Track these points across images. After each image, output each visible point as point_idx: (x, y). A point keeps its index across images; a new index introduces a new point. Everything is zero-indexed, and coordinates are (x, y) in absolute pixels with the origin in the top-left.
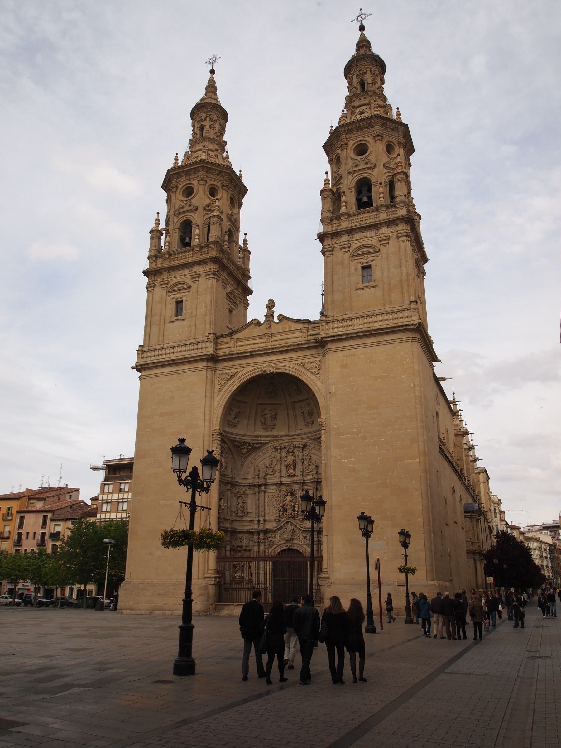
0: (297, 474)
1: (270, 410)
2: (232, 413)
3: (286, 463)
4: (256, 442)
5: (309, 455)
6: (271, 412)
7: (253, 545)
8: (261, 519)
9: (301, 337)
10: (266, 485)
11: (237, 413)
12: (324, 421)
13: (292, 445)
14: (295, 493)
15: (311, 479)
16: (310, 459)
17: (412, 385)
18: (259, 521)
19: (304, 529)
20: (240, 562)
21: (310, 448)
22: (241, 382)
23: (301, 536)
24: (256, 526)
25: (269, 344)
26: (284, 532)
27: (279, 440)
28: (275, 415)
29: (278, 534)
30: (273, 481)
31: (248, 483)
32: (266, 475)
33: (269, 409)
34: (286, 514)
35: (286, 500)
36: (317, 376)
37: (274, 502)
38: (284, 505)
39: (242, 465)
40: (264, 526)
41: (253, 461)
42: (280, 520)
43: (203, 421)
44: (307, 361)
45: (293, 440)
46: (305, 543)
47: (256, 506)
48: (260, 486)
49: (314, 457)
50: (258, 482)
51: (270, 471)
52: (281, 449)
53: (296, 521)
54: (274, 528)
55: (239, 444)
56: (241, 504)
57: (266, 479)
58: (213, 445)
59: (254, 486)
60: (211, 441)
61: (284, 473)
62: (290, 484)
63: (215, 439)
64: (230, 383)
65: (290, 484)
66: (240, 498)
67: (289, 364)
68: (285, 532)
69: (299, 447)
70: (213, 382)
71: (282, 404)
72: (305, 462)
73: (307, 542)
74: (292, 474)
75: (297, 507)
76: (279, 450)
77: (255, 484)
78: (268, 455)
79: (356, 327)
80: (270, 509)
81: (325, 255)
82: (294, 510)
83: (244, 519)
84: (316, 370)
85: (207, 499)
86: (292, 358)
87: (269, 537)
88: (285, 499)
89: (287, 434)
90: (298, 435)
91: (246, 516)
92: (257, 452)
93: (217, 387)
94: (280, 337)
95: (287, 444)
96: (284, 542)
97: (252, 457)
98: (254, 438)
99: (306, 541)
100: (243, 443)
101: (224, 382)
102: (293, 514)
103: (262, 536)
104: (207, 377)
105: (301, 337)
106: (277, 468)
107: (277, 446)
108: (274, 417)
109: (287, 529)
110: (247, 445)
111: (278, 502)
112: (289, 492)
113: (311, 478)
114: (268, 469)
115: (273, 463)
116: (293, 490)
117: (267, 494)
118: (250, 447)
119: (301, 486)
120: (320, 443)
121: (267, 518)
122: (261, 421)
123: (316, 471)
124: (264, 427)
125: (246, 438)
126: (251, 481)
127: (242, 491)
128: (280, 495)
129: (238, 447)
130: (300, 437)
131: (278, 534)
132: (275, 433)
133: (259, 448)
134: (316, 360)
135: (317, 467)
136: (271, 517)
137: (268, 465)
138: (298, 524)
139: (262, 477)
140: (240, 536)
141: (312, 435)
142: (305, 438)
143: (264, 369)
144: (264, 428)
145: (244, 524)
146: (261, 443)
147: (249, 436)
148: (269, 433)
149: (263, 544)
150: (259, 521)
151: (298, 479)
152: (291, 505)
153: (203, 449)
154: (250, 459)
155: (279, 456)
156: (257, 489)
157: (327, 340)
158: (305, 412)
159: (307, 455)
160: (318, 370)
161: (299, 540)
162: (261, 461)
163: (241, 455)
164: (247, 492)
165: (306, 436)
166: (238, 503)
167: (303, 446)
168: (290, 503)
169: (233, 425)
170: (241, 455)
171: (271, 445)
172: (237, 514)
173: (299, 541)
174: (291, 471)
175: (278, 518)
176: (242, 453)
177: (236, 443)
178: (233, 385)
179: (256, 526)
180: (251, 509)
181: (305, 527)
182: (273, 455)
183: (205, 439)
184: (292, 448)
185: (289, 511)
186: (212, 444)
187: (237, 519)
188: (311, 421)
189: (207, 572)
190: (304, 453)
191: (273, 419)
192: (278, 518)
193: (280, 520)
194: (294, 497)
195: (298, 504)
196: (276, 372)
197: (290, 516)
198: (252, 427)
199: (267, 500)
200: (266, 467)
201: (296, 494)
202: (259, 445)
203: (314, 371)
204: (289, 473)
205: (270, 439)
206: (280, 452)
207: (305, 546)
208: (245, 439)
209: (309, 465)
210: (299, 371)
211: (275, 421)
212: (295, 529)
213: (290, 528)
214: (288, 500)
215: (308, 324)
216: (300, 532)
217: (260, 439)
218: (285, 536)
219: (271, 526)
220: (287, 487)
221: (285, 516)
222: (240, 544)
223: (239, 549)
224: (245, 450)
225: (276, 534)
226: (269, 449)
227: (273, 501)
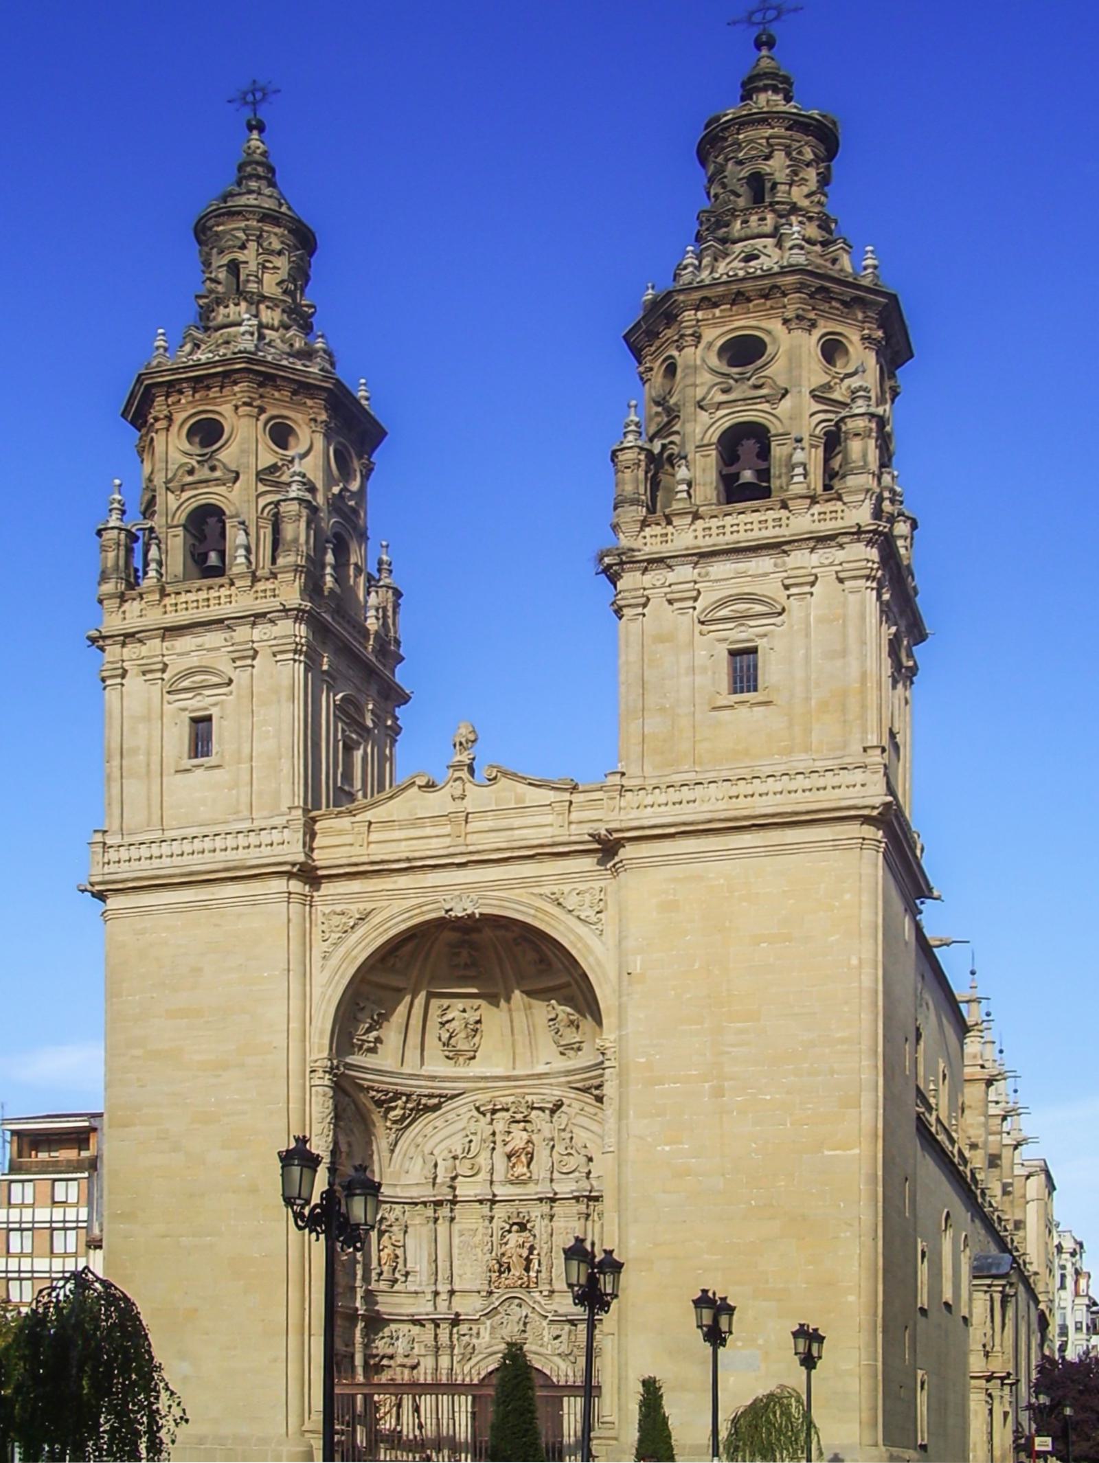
3: (508, 1149)
4: (426, 1092)
5: (568, 1129)
7: (423, 1352)
8: (443, 1288)
9: (551, 825)
10: (454, 1202)
13: (523, 1101)
15: (572, 1192)
17: (854, 961)
20: (390, 1394)
21: (572, 1111)
23: (545, 1333)
24: (429, 1307)
25: (461, 840)
26: (502, 1323)
28: (479, 1022)
29: (486, 1328)
30: (472, 1193)
32: (454, 1178)
33: (461, 1007)
34: (506, 1279)
35: (506, 1244)
37: (476, 1247)
38: (503, 1255)
39: (392, 1151)
40: (449, 1308)
41: (419, 1140)
42: (491, 1293)
46: (557, 1352)
47: (430, 1255)
48: (438, 1204)
49: (581, 1136)
50: (434, 1196)
51: (463, 1168)
52: (494, 1112)
53: (533, 1297)
55: (383, 1098)
57: (453, 1188)
59: (424, 1203)
67: (516, 895)
69: (542, 1109)
75: (536, 1262)
76: (488, 1115)
78: (460, 1125)
79: (705, 807)
80: (465, 1264)
81: (623, 616)
83: (397, 1287)
87: (464, 1335)
88: (505, 1240)
90: (539, 1076)
94: (490, 824)
95: (511, 1099)
100: (391, 1094)
102: (526, 1279)
105: (551, 825)
106: (483, 1160)
107: (483, 1105)
108: (475, 1029)
110: (404, 1098)
111: (487, 1248)
113: (574, 1188)
114: (457, 1162)
115: (472, 1149)
116: (527, 1218)
117: (456, 1227)
119: (545, 1208)
120: (599, 1099)
123: (586, 1170)
124: (447, 1053)
126: (414, 1193)
127: (392, 1217)
131: (486, 1328)
133: (436, 1107)
134: (592, 888)
136: (468, 1287)
137: (459, 1152)
138: (539, 1303)
139: (443, 1184)
141: (577, 1077)
142: (559, 1085)
144: (448, 1057)
146: (440, 1096)
147: (412, 1076)
148: (462, 1071)
150: (436, 1294)
151: (539, 1189)
152: (521, 1256)
154: (413, 1135)
155: (490, 1129)
157: (624, 838)
159: (564, 1130)
161: (540, 1342)
162: (442, 1141)
166: (381, 1247)
167: (554, 1105)
173: (542, 1346)
174: (521, 1169)
175: (487, 1288)
181: (556, 1311)
182: (473, 1127)
185: (517, 1271)
190: (556, 1124)
192: (487, 1288)
194: (526, 1234)
195: (539, 1254)
197: (520, 1282)
199: (456, 1241)
200: (455, 1158)
201: (533, 1227)
202: (436, 1101)
204: (516, 1174)
206: (492, 1120)
207: (557, 1359)
210: (546, 912)
211: (476, 1039)
212: (530, 1315)
213: (517, 1312)
214: (512, 1244)
215: (572, 793)
216: (545, 1323)
219: (467, 1306)
220: (511, 1210)
221: (507, 1282)
224: (398, 1112)
225: (482, 1327)
226: (461, 1112)
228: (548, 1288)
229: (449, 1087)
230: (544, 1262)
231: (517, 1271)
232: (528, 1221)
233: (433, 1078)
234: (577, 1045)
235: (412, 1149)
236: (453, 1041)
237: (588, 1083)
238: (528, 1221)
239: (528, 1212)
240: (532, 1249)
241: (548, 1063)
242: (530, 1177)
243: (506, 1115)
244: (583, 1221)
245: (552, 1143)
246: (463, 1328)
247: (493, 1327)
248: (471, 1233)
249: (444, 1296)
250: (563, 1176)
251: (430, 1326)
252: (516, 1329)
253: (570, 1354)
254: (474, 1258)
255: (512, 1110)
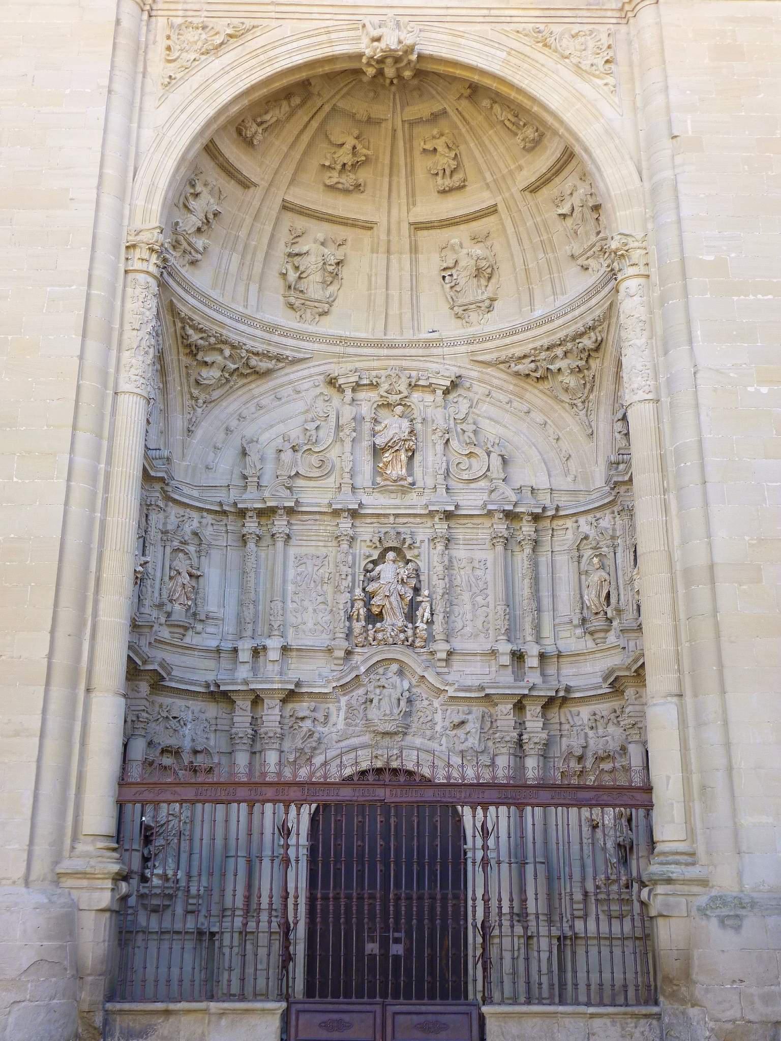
0: (420, 484)
1: (323, 244)
2: (193, 204)
4: (260, 347)
5: (470, 420)
6: (326, 251)
11: (211, 216)
12: (636, 244)
14: (416, 552)
16: (475, 432)
18: (257, 652)
19: (456, 690)
22: (268, 71)
23: (438, 718)
27: (350, 355)
28: (338, 264)
31: (212, 503)
33: (321, 236)
36: (600, 82)
37: (323, 583)
41: (233, 423)
42: (349, 653)
43: (95, 182)
44: (557, 29)
45: (404, 363)
48: (266, 513)
49: (491, 430)
54: (328, 682)
55: (201, 342)
56: (186, 579)
58: (129, 290)
60: (123, 271)
61: (365, 477)
62: (392, 519)
63: (138, 265)
64: (216, 64)
65: (392, 519)
66: (181, 555)
68: (375, 701)
70: (140, 52)
71: (368, 226)
72: (454, 443)
73: (469, 744)
74: (402, 483)
75: (426, 606)
76: (349, 392)
77: (249, 506)
78: (300, 406)
82: (411, 616)
84: (600, 62)
85: (93, 510)
86: (493, 12)
87: (303, 719)
88: (374, 573)
89: (379, 335)
90: (428, 344)
91: (199, 627)
92: (256, 392)
93: (158, 68)
96: (366, 738)
97: (231, 409)
98: (258, 333)
99: (466, 739)
100: (212, 340)
101: (193, 56)
102: (410, 632)
103: (271, 714)
104: (118, 22)
109: (384, 687)
110: (227, 352)
112: (391, 549)
116: (408, 542)
117: (292, 551)
118: (234, 367)
119: (442, 527)
121: (293, 640)
122: (284, 275)
124: (292, 300)
125: (228, 321)
127: (187, 529)
128: (350, 558)
129: (192, 350)
130: (435, 351)
131: (339, 710)
132: (327, 326)
133: (266, 374)
135: (505, 461)
136: (307, 641)
140: (178, 705)
143: (376, 33)
144: (291, 306)
145: (189, 660)
146: (278, 358)
149: (277, 746)
150: (257, 652)
153: (88, 295)
155: (348, 413)
156: (251, 525)
158: (462, 263)
160: (607, 61)
162: (272, 426)
163: (195, 392)
164: (208, 533)
165: (463, 349)
168: (399, 587)
169: (188, 257)
170: (195, 392)
171: (313, 371)
172: (169, 615)
174: (398, 470)
176: (197, 383)
177: (190, 332)
178: (233, 74)
179: (243, 672)
180: (219, 607)
183: (100, 253)
184: (403, 387)
185: (394, 620)
186: (125, 287)
187: (165, 633)
188: (484, 297)
189: (73, 848)
191: (329, 279)
192: (345, 644)
193: (349, 653)
194: (410, 565)
196: (420, 57)
197: (402, 636)
198: (254, 288)
199: (291, 573)
202: (270, 365)
203: (589, 62)
205: (316, 346)
208: (222, 325)
209: (470, 455)
216: (436, 703)
217: (276, 338)
218: (374, 713)
220: (384, 530)
221: (380, 636)
222: (172, 741)
223: (167, 761)
224: (215, 373)
225: (333, 707)
227: (318, 580)
228: (447, 647)
229: (289, 346)
230: (439, 609)
231: (394, 620)
232: (410, 547)
233: (272, 328)
234: (487, 303)
235: (222, 435)
236: (302, 285)
237: (503, 355)
238: (410, 548)
239: (412, 533)
240: (417, 590)
241: (433, 332)
242: (413, 484)
243: (373, 395)
244: (500, 548)
245: (447, 436)
246: (302, 708)
247: (350, 707)
248: (318, 562)
249: (274, 655)
250: (461, 486)
251: (244, 704)
252: (396, 711)
253: (482, 752)
254: (320, 599)
255: (385, 386)
